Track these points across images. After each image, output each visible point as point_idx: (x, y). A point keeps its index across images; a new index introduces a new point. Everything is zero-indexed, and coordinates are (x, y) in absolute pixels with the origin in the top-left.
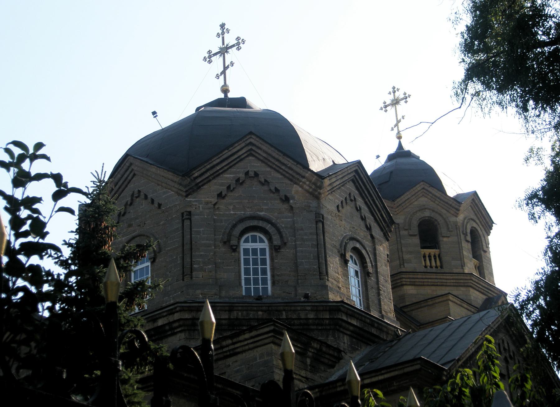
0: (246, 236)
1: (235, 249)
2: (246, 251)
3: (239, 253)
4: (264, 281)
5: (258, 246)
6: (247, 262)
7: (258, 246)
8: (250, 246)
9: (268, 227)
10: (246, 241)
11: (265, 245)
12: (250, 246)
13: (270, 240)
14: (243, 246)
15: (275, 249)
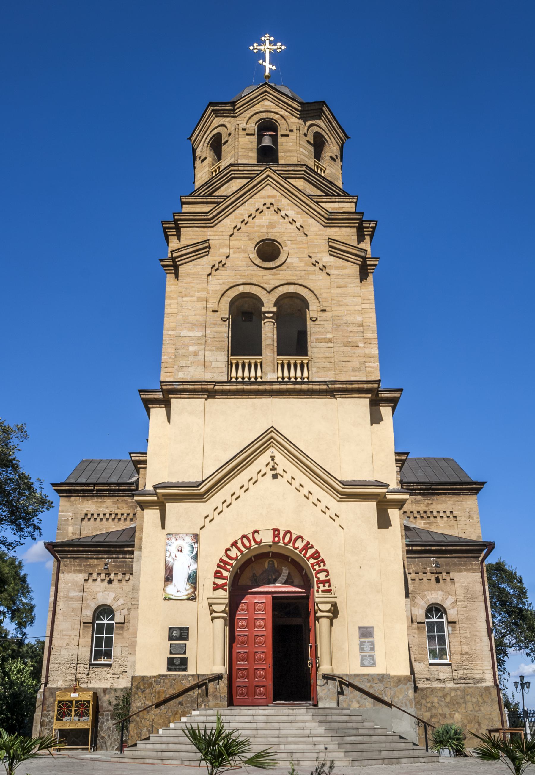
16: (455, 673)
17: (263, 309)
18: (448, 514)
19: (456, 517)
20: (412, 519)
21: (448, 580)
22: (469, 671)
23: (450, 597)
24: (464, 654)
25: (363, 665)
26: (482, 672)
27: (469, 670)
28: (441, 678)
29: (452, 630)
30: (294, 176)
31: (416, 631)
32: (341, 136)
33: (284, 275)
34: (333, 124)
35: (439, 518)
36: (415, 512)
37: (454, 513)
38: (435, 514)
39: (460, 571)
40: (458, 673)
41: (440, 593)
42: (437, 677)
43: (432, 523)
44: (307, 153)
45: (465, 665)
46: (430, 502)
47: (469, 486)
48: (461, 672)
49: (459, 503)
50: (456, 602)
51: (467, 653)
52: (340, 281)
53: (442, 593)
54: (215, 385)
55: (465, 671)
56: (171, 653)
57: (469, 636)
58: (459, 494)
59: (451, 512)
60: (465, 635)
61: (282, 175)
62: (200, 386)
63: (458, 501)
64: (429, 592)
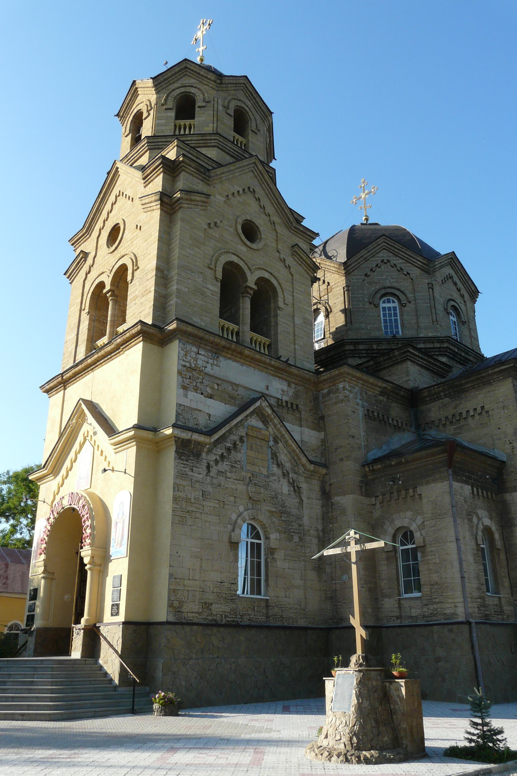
0: (384, 299)
1: (377, 306)
2: (384, 309)
3: (380, 308)
4: (397, 327)
5: (391, 305)
6: (385, 315)
7: (391, 305)
8: (387, 305)
9: (397, 293)
10: (384, 302)
11: (396, 304)
12: (387, 305)
13: (399, 300)
14: (382, 305)
15: (402, 305)
16: (425, 609)
17: (105, 291)
18: (479, 410)
19: (487, 412)
20: (441, 427)
21: (417, 496)
22: (439, 606)
23: (419, 517)
24: (433, 585)
25: (112, 615)
26: (453, 605)
27: (440, 604)
28: (413, 615)
29: (422, 557)
30: (143, 152)
31: (386, 562)
32: (213, 78)
33: (121, 250)
34: (202, 73)
35: (470, 419)
36: (443, 419)
37: (486, 407)
38: (464, 415)
39: (428, 483)
40: (428, 609)
41: (409, 514)
42: (409, 614)
43: (462, 425)
44: (164, 121)
45: (435, 599)
46: (458, 402)
47: (496, 370)
48: (431, 607)
49: (491, 393)
50: (423, 522)
51: (437, 583)
52: (147, 234)
53: (411, 513)
54: (62, 377)
55: (435, 606)
56: (29, 611)
57: (438, 562)
58: (489, 383)
59: (483, 408)
60: (434, 561)
61: (191, 145)
62: (55, 381)
63: (489, 392)
64: (398, 515)
